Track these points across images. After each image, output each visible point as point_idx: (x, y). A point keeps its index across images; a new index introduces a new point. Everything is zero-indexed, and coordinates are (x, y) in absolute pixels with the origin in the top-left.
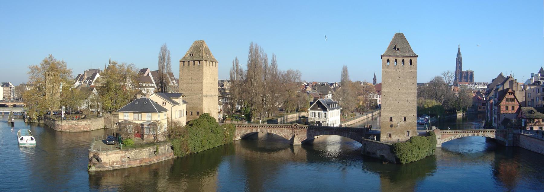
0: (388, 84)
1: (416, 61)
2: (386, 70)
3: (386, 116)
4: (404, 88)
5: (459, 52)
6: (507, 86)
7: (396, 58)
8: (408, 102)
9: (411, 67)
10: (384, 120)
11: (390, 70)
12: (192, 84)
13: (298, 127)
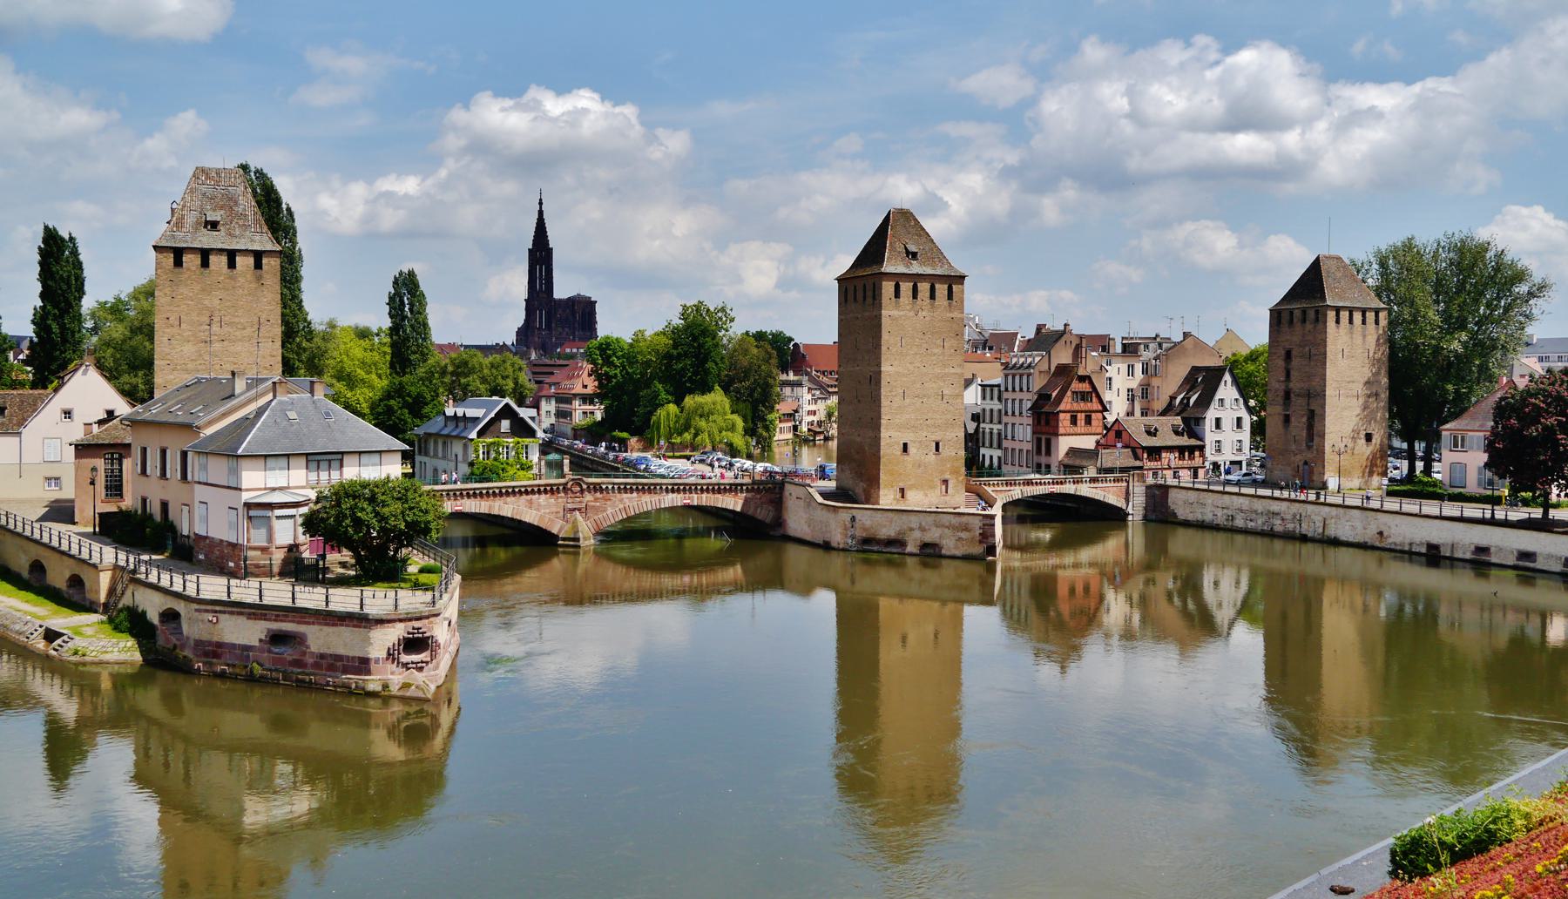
0: (897, 351)
2: (891, 313)
4: (934, 362)
6: (1062, 356)
8: (945, 401)
9: (950, 303)
10: (888, 451)
11: (901, 313)
12: (225, 343)
13: (585, 486)
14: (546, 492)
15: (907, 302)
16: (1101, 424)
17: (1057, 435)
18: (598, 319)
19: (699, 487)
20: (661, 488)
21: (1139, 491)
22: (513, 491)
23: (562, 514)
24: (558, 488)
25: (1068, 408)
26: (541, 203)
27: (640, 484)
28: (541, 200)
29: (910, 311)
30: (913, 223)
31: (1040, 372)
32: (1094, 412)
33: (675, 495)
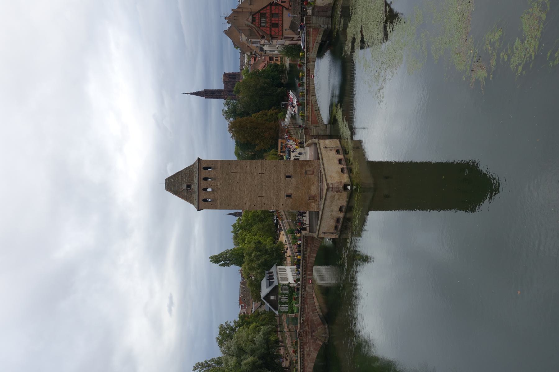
1: (206, 160)
2: (219, 204)
3: (284, 203)
4: (244, 178)
5: (197, 94)
7: (201, 189)
14: (303, 348)
15: (213, 195)
16: (278, 7)
17: (283, 35)
18: (231, 72)
19: (304, 276)
20: (303, 294)
21: (315, 21)
22: (302, 363)
23: (313, 340)
24: (302, 343)
25: (268, 29)
26: (187, 94)
27: (301, 305)
28: (186, 94)
29: (217, 193)
30: (172, 180)
31: (250, 35)
32: (271, 11)
33: (307, 287)
